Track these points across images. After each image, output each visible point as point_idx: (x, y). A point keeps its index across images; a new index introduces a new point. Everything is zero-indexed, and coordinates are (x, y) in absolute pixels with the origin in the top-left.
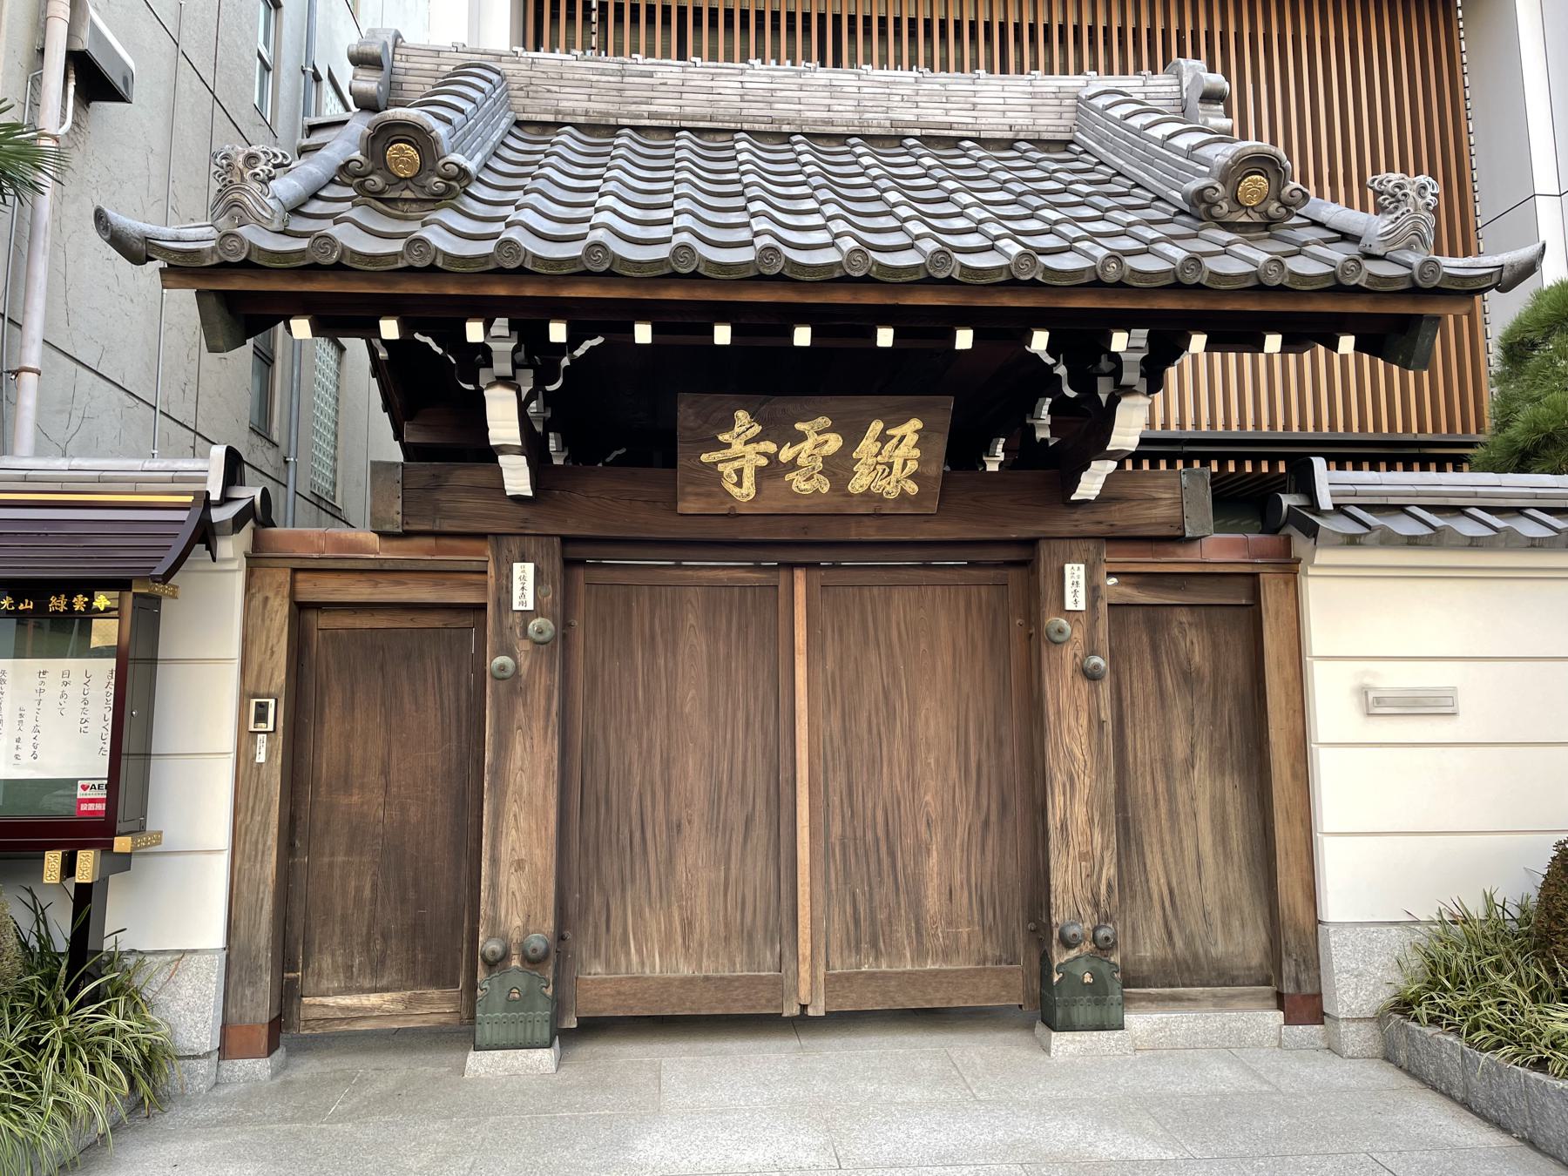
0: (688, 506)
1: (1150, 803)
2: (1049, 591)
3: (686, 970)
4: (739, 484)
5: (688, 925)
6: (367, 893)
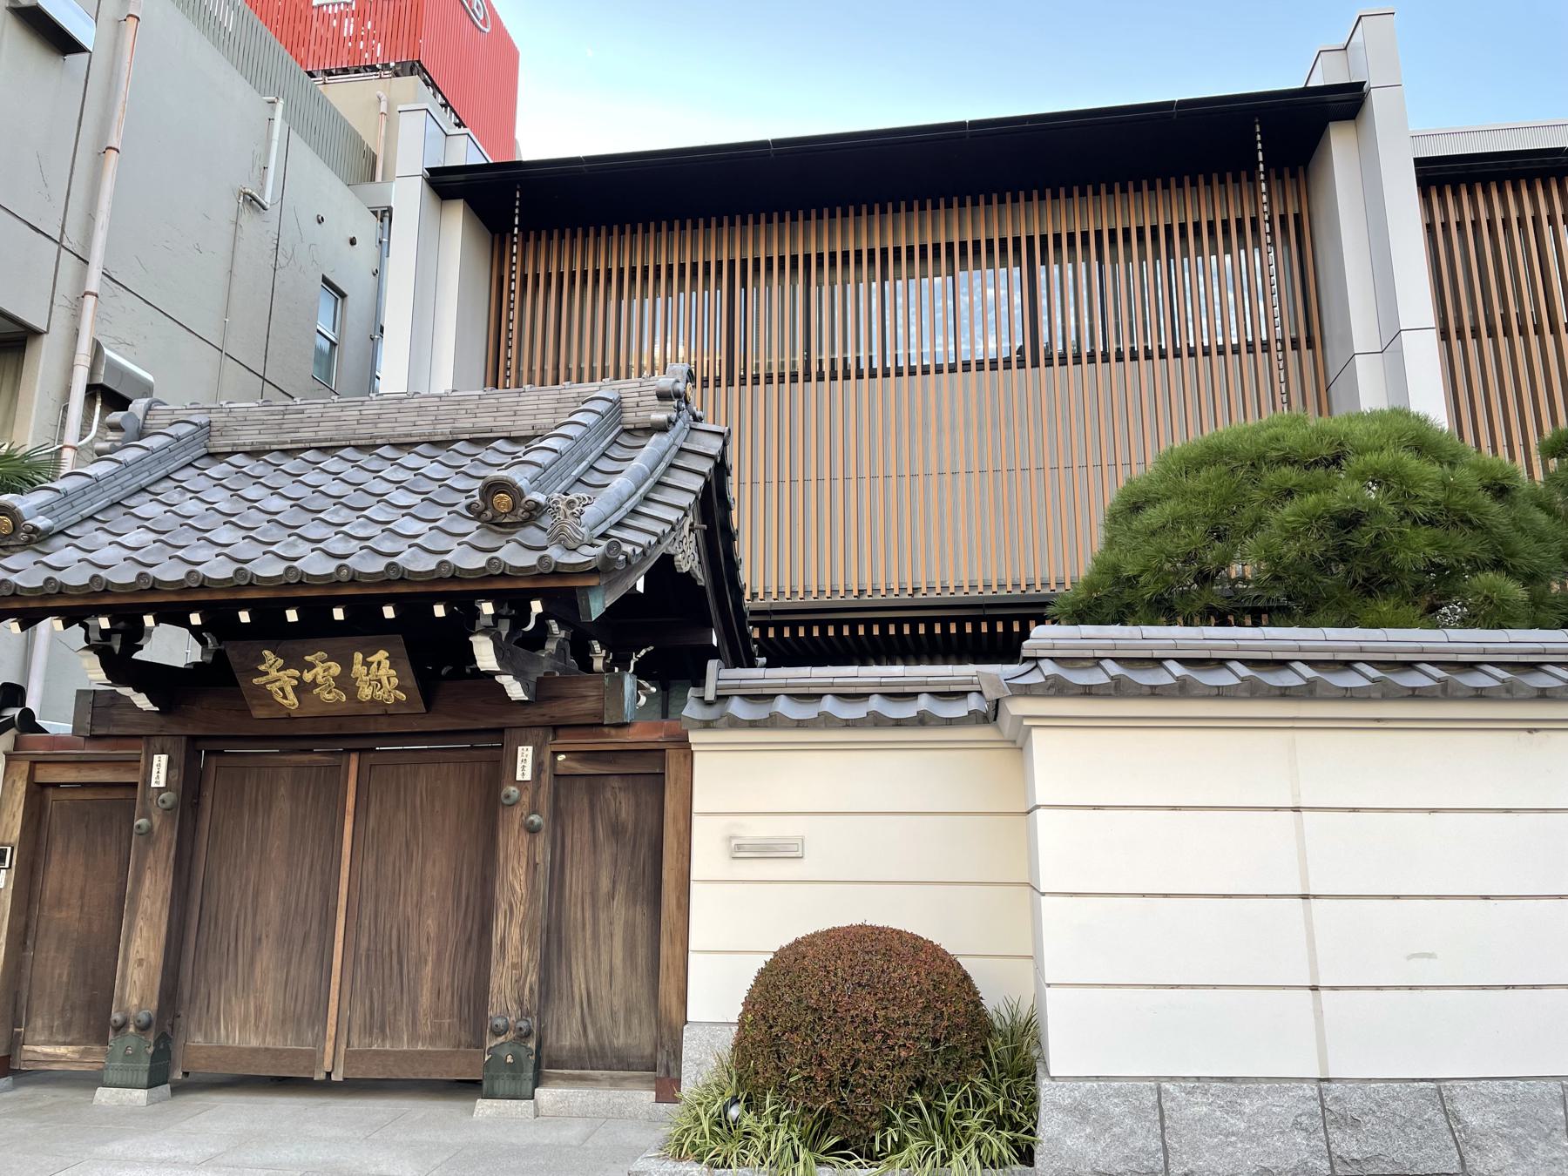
0: (259, 713)
1: (579, 926)
2: (509, 767)
3: (254, 1043)
4: (285, 697)
5: (259, 1010)
6: (65, 978)
